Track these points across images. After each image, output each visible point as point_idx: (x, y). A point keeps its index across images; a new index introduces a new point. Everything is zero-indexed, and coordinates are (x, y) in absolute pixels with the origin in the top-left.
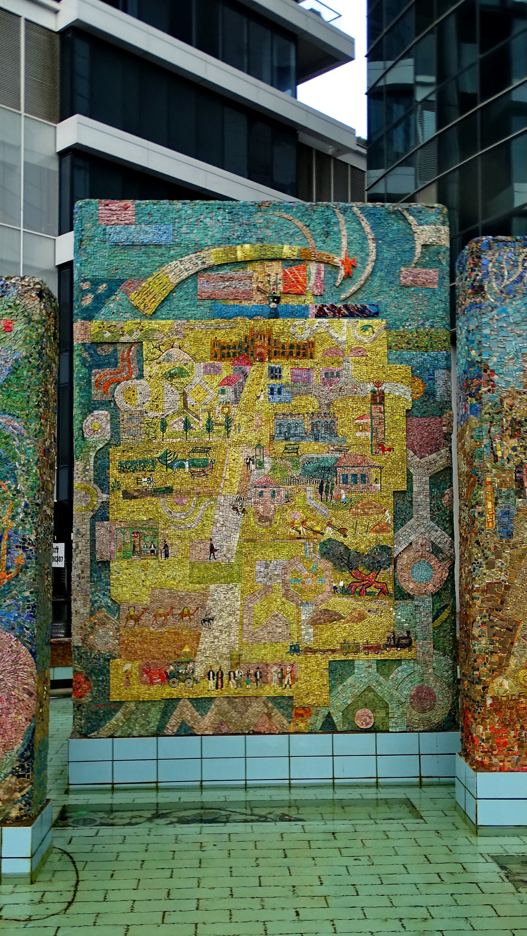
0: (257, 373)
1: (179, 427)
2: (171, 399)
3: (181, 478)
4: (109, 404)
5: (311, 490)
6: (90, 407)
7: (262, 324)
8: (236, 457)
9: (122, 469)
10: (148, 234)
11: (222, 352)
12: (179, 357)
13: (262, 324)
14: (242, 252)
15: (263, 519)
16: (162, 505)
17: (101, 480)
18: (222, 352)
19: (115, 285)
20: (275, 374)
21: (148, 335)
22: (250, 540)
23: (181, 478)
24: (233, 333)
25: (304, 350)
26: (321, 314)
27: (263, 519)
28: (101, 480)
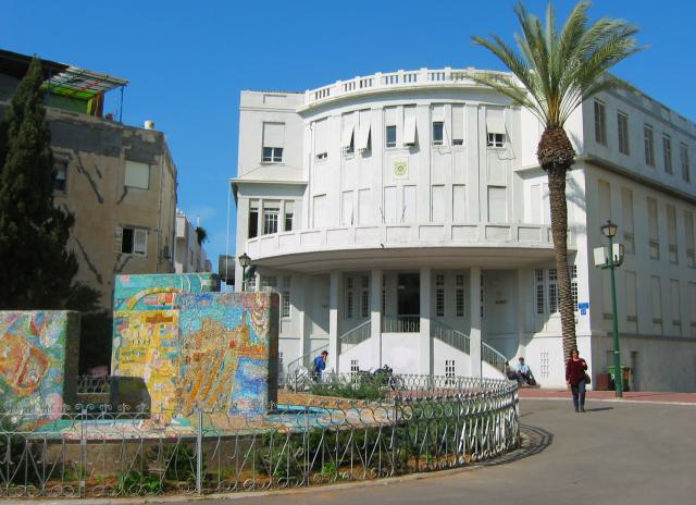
0: (158, 325)
1: (136, 342)
2: (135, 336)
3: (137, 357)
4: (120, 335)
5: (170, 362)
6: (116, 336)
7: (159, 311)
8: (152, 351)
9: (123, 354)
10: (133, 285)
11: (149, 320)
12: (138, 322)
13: (159, 311)
14: (156, 289)
15: (157, 370)
16: (131, 365)
17: (117, 357)
18: (149, 320)
19: (123, 300)
20: (162, 326)
21: (130, 315)
22: (153, 376)
23: (137, 357)
24: (152, 315)
25: (170, 319)
26: (174, 308)
27: (157, 370)
28: (117, 357)
